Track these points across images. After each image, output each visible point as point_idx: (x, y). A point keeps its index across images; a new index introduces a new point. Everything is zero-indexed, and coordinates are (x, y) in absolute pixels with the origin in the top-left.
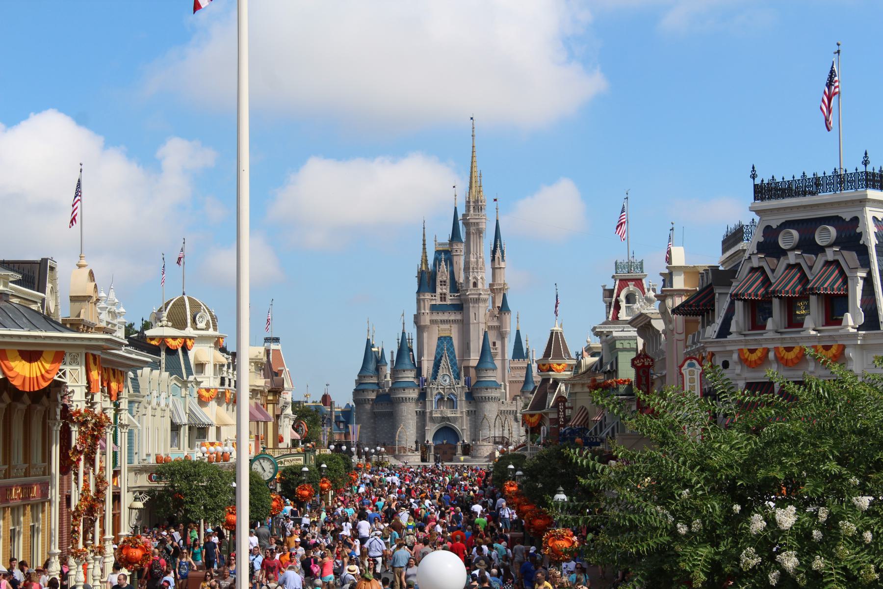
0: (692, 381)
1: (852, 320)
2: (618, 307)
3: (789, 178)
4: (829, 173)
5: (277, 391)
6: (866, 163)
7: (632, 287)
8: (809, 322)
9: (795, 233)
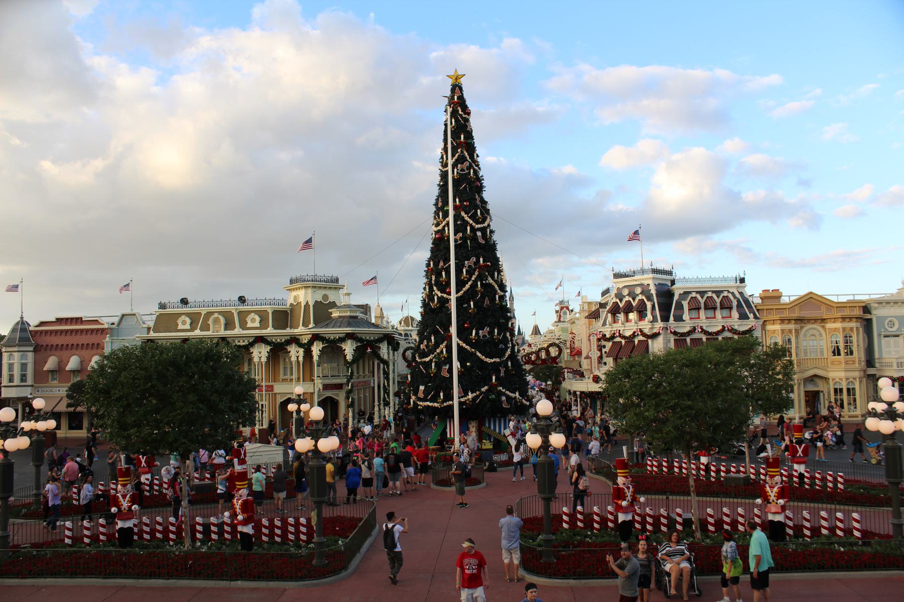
4: (639, 269)
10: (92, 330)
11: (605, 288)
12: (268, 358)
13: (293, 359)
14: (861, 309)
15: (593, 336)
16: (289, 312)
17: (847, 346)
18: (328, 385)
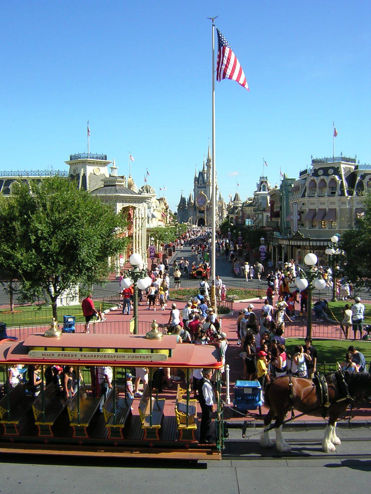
3: (321, 158)
4: (332, 157)
5: (167, 209)
6: (341, 155)
11: (303, 170)
15: (295, 204)
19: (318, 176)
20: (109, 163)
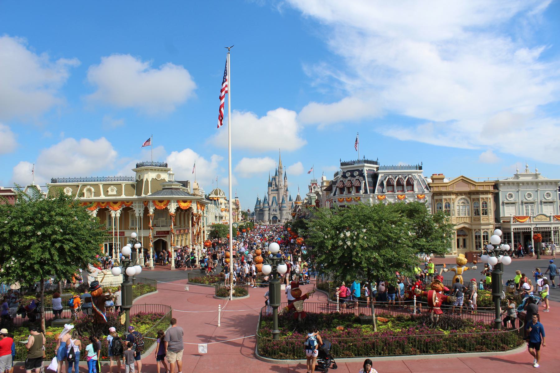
0: (328, 205)
1: (362, 192)
2: (312, 190)
4: (357, 160)
5: (238, 209)
7: (315, 185)
8: (353, 192)
9: (350, 173)
10: (7, 196)
11: (336, 172)
12: (121, 214)
13: (137, 215)
14: (492, 187)
15: (328, 202)
16: (135, 185)
17: (483, 209)
18: (160, 232)
19: (346, 177)
20: (169, 170)
